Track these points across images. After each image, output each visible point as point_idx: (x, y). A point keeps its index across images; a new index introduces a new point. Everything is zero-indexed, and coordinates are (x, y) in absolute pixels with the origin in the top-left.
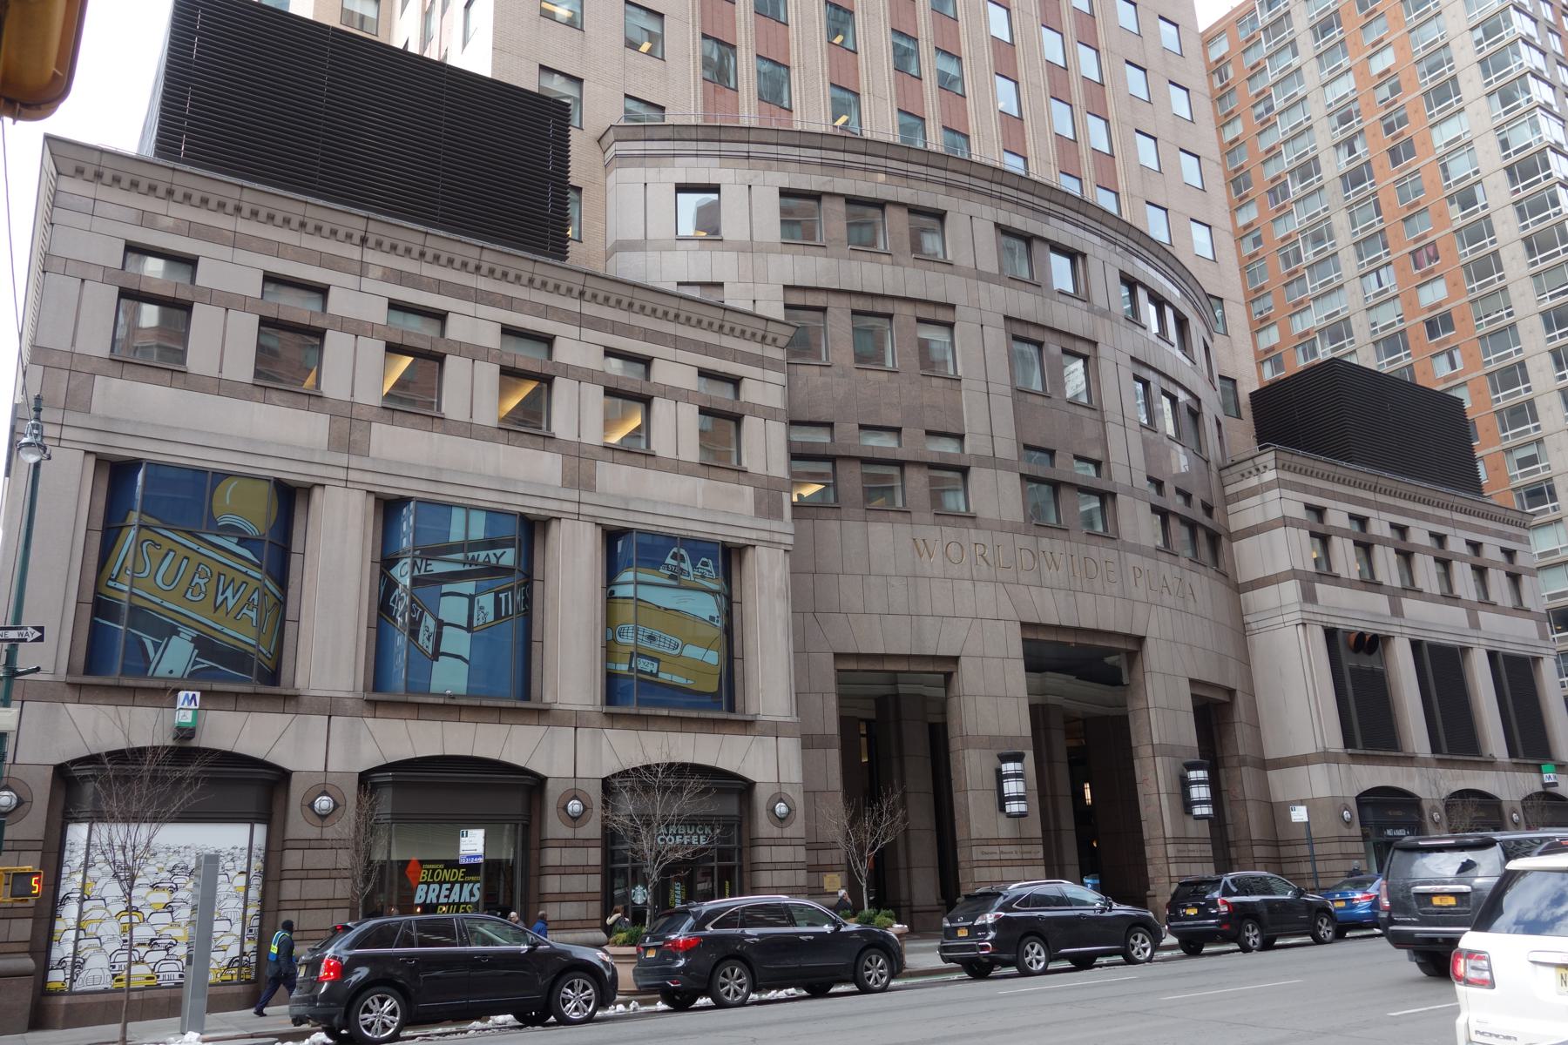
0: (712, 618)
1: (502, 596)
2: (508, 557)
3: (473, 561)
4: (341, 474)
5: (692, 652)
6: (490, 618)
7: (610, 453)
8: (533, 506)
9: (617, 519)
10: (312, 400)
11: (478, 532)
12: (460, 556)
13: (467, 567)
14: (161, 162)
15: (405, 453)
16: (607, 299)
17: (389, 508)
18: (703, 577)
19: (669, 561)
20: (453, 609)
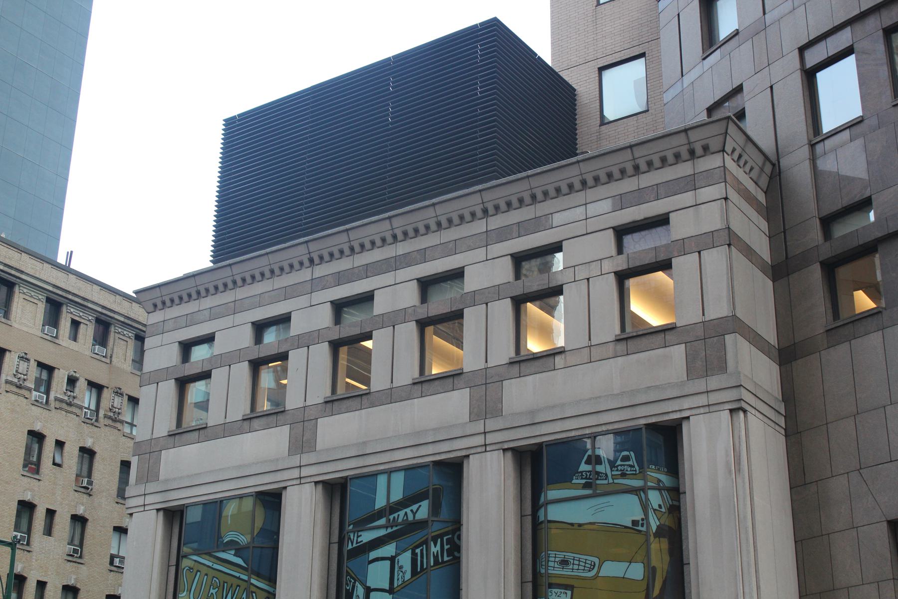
0: (635, 523)
1: (418, 551)
2: (423, 510)
3: (395, 523)
4: (295, 473)
5: (612, 569)
6: (408, 576)
7: (516, 368)
8: (445, 451)
9: (525, 437)
10: (280, 417)
11: (397, 495)
12: (383, 521)
13: (390, 530)
14: (220, 265)
15: (344, 436)
16: (462, 218)
17: (336, 491)
18: (623, 475)
19: (584, 467)
20: (378, 575)
